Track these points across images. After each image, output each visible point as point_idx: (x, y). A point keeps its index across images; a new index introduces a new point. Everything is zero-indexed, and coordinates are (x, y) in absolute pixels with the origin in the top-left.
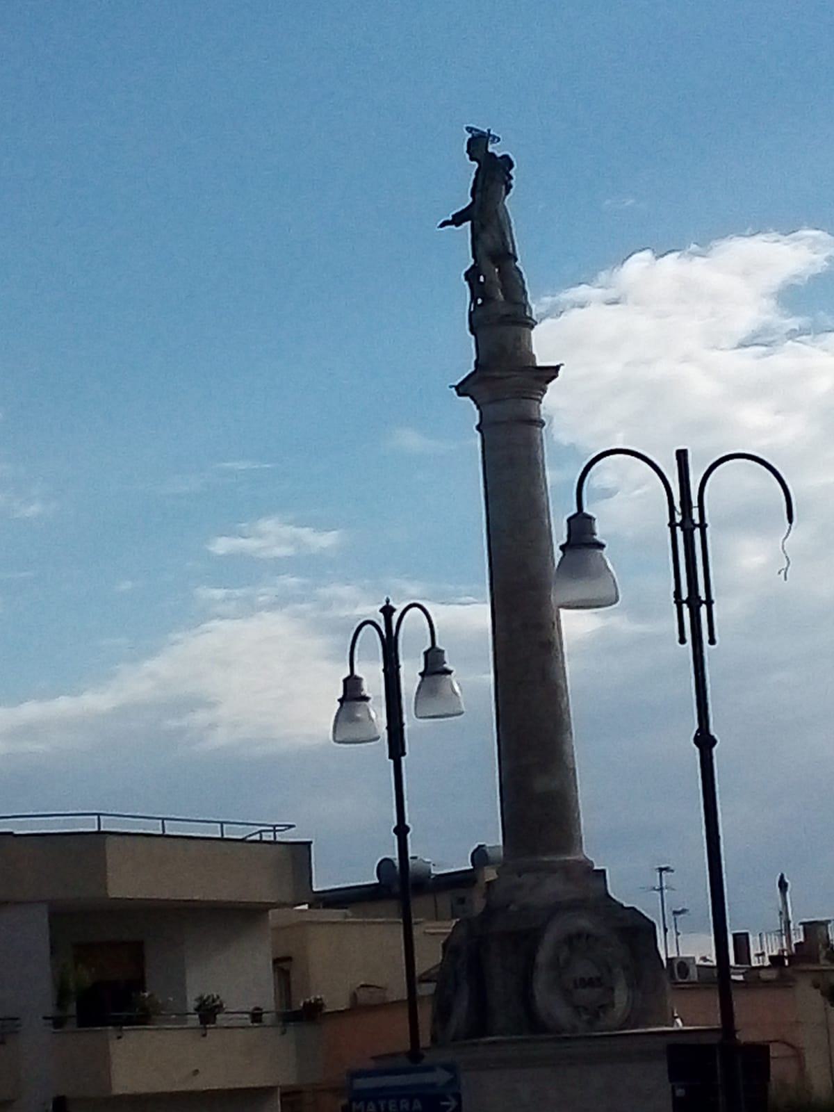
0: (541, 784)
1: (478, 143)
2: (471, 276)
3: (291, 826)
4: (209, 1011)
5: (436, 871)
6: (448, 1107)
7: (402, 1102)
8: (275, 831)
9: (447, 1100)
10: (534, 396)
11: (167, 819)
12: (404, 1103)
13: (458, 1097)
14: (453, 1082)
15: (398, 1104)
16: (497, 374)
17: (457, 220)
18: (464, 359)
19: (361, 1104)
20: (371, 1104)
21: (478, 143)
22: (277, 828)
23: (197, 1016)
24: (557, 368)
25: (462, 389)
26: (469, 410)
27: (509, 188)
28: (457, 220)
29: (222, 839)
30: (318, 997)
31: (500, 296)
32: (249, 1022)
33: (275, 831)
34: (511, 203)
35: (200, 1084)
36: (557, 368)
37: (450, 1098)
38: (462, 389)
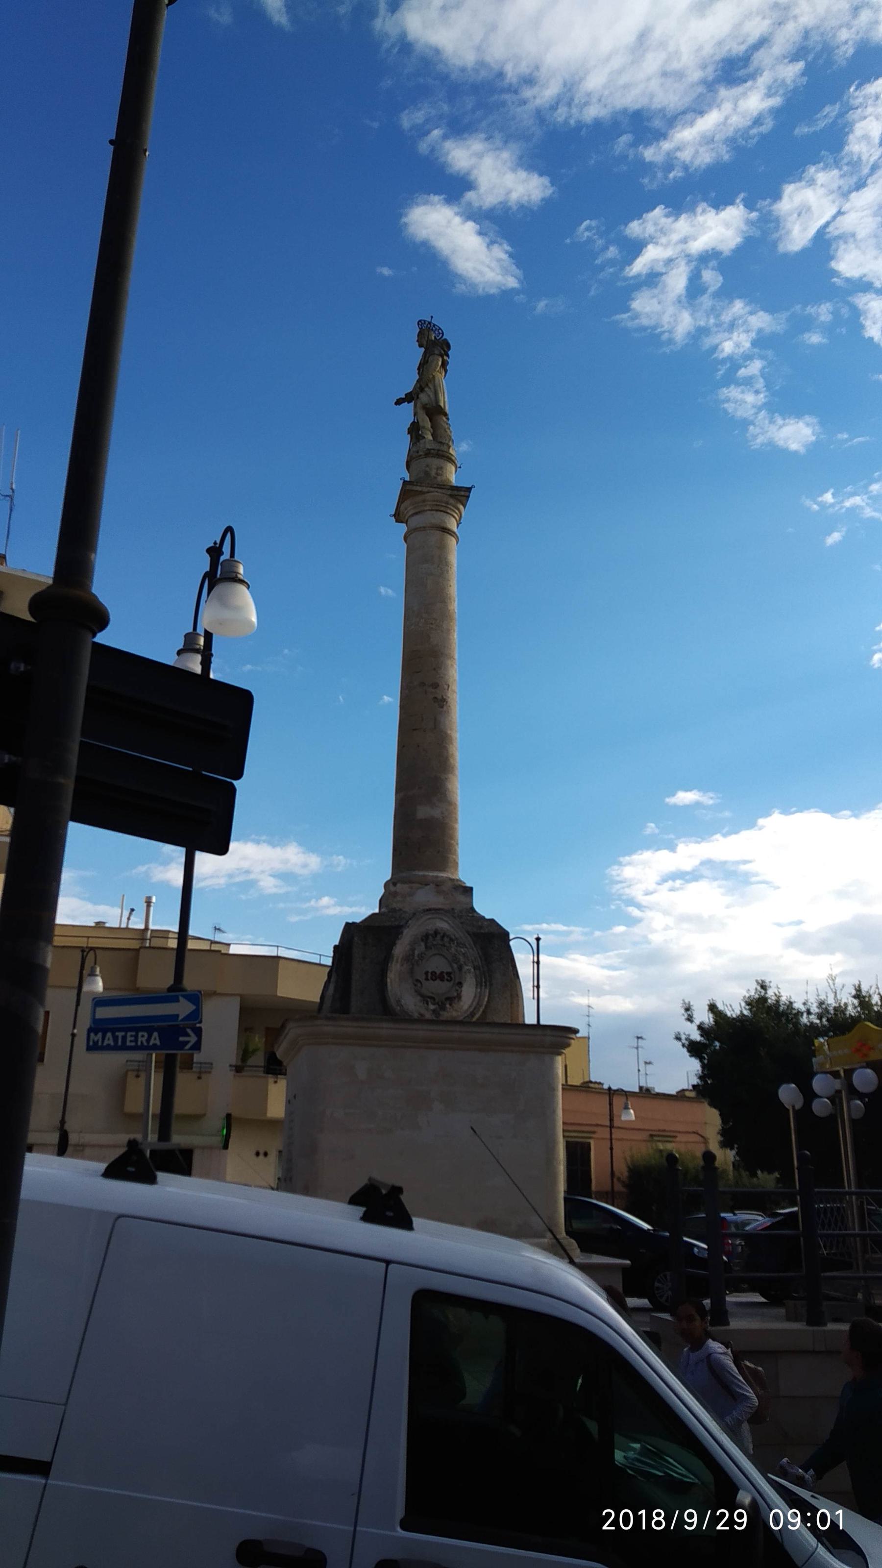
0: (423, 812)
6: (187, 1042)
7: (140, 1034)
9: (188, 1035)
10: (449, 511)
12: (143, 1036)
13: (198, 1032)
14: (196, 1015)
15: (136, 1037)
16: (419, 488)
19: (100, 1035)
20: (109, 1035)
24: (469, 490)
31: (430, 437)
36: (469, 490)
37: (189, 1031)
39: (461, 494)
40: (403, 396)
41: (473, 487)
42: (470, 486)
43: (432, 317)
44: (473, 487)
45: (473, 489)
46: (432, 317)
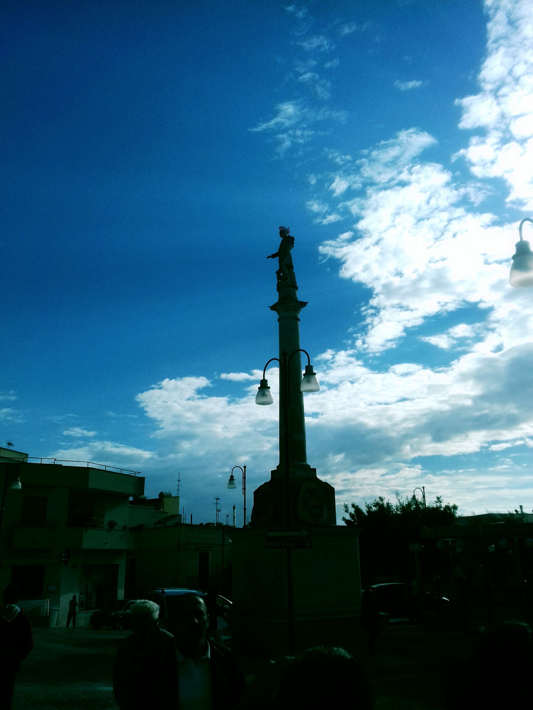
1: (283, 232)
2: (278, 273)
3: (140, 473)
4: (112, 525)
5: (148, 498)
8: (135, 474)
11: (107, 466)
17: (273, 256)
18: (275, 298)
21: (283, 232)
22: (136, 473)
23: (108, 526)
24: (306, 303)
25: (273, 308)
26: (275, 315)
27: (293, 246)
28: (273, 256)
29: (121, 474)
30: (143, 523)
32: (122, 529)
33: (135, 474)
34: (293, 251)
35: (107, 547)
36: (306, 303)
38: (273, 308)
39: (304, 304)
40: (271, 255)
41: (308, 302)
42: (307, 302)
43: (289, 227)
44: (308, 302)
45: (308, 303)
46: (289, 227)
